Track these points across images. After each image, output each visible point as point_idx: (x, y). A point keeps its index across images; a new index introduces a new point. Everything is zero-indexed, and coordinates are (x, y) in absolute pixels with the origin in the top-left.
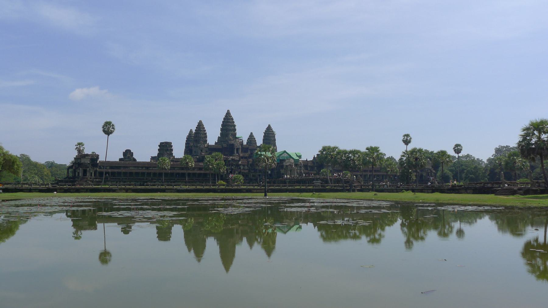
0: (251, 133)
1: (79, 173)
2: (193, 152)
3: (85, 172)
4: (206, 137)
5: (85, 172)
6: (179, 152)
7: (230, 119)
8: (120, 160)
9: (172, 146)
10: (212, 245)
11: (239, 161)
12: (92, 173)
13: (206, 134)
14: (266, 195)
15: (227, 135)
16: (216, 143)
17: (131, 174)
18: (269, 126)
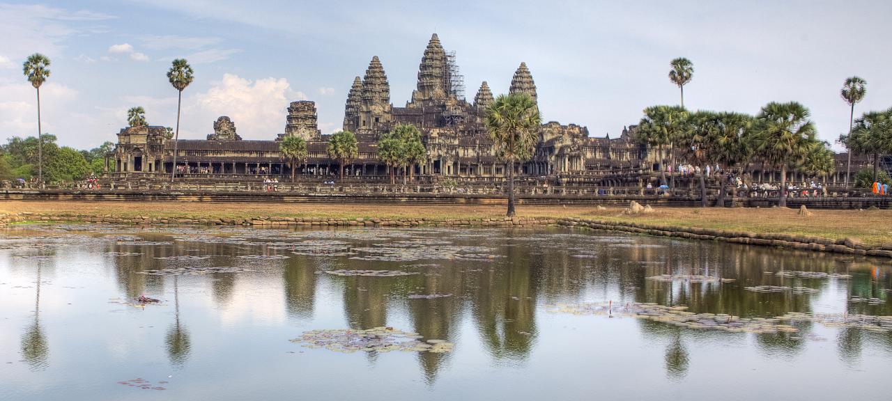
0: (484, 83)
1: (125, 164)
2: (361, 123)
3: (138, 163)
4: (387, 91)
5: (138, 163)
6: (331, 122)
7: (437, 53)
8: (210, 137)
9: (314, 110)
10: (399, 321)
11: (454, 138)
12: (150, 164)
13: (386, 84)
14: (511, 209)
15: (431, 87)
16: (408, 104)
17: (228, 166)
18: (523, 64)
